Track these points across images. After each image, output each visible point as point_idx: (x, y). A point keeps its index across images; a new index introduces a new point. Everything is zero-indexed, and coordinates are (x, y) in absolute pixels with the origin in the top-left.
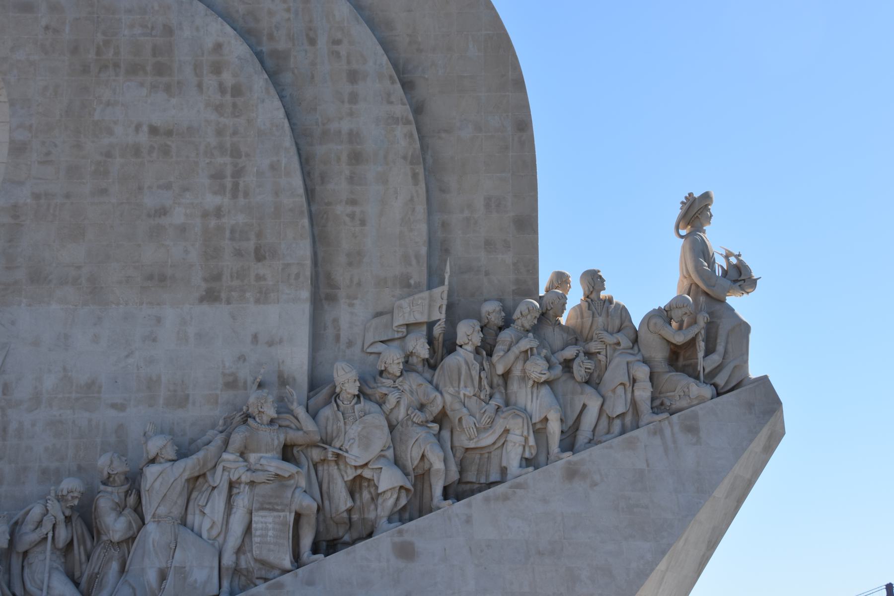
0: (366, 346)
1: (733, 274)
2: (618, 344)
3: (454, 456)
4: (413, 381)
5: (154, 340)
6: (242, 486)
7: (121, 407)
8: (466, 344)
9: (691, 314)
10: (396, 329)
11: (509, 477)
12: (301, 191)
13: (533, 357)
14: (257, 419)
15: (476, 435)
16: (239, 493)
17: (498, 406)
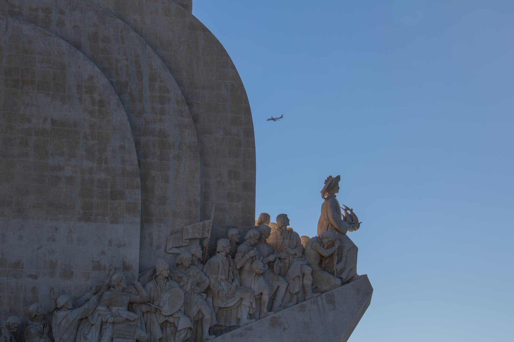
0: (167, 249)
1: (349, 220)
2: (296, 254)
3: (214, 311)
4: (194, 271)
5: (54, 240)
6: (108, 324)
7: (35, 277)
8: (222, 252)
9: (332, 241)
10: (184, 241)
11: (241, 324)
12: (136, 162)
13: (256, 260)
14: (117, 289)
15: (226, 301)
16: (106, 328)
17: (237, 285)
